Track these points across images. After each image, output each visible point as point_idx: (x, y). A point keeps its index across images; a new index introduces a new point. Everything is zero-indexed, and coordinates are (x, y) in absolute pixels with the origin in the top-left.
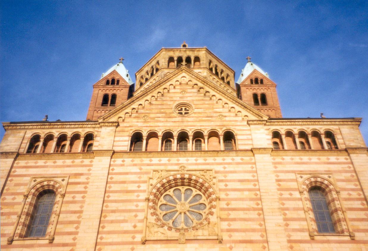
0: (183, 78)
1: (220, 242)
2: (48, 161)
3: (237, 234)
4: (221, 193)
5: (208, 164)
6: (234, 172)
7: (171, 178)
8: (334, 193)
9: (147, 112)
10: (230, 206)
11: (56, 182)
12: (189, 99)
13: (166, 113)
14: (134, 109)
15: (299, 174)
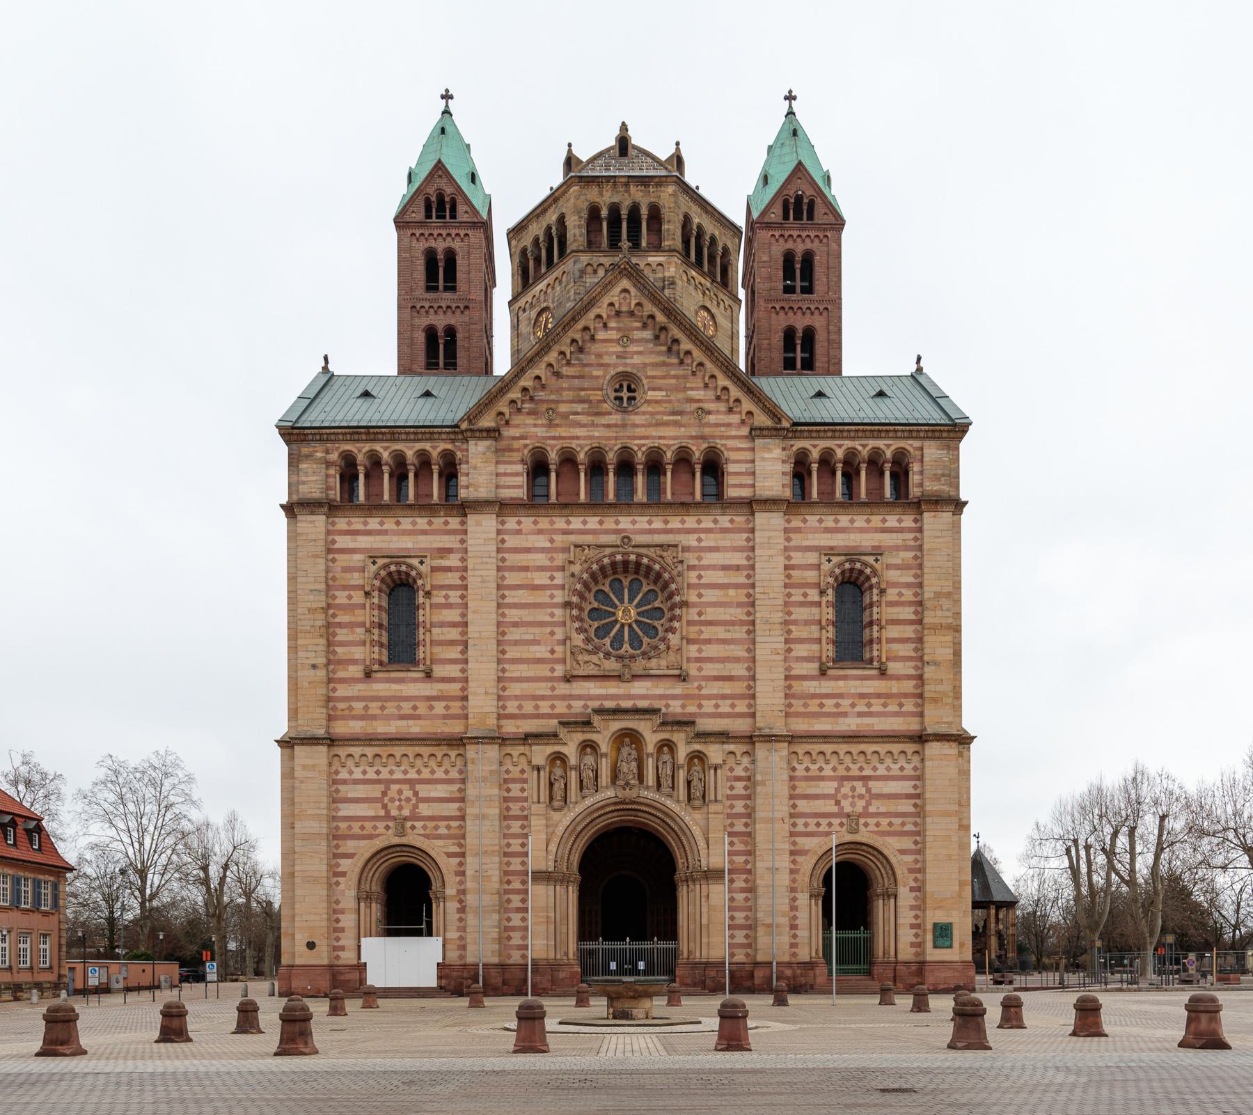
0: (623, 295)
1: (684, 680)
2: (384, 520)
3: (710, 665)
4: (691, 591)
5: (670, 531)
6: (716, 549)
7: (606, 561)
8: (875, 591)
9: (553, 397)
10: (703, 618)
11: (410, 566)
12: (637, 360)
13: (590, 402)
14: (525, 390)
15: (825, 555)
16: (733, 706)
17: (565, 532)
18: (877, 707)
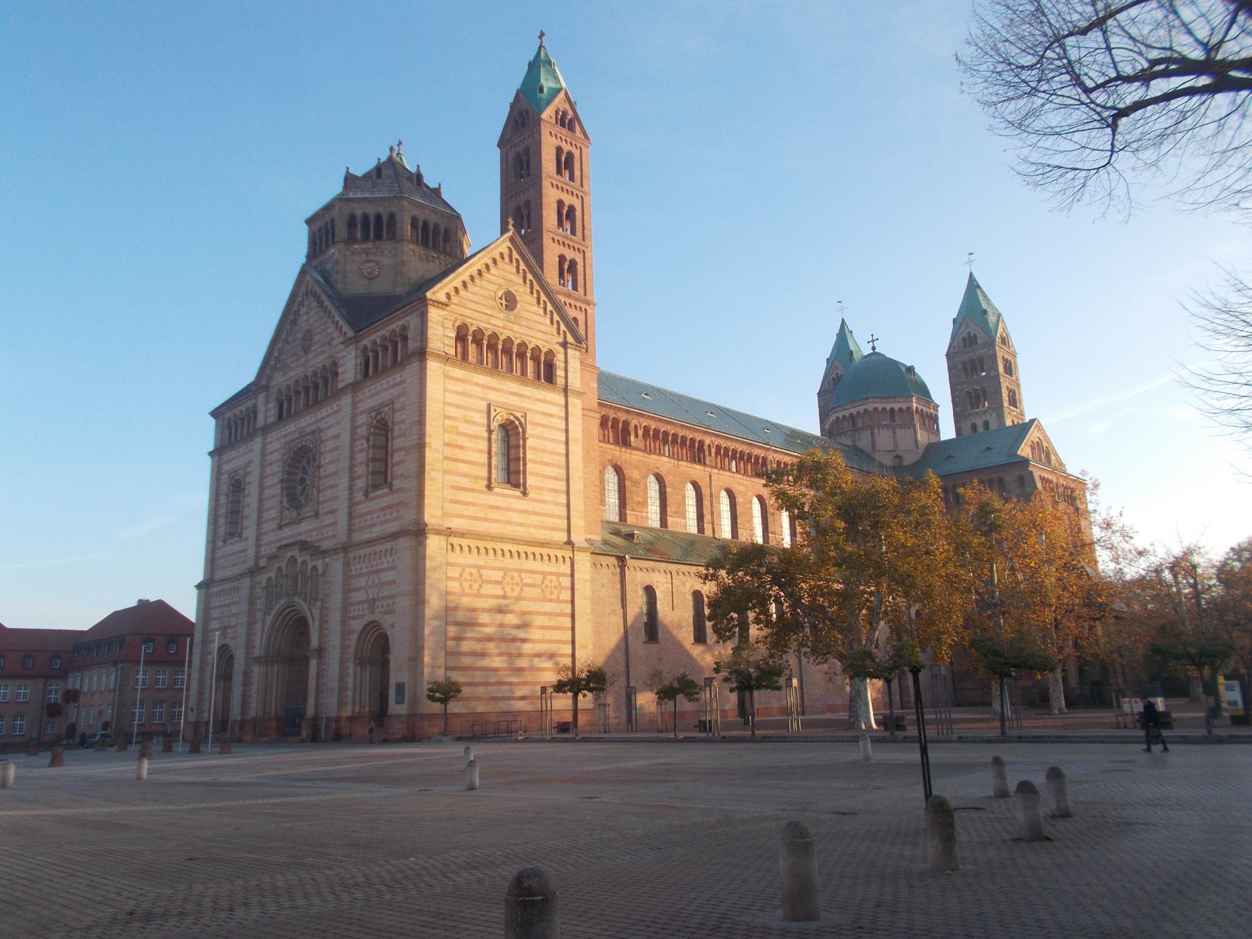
14: (276, 358)
16: (334, 530)
17: (285, 436)
18: (388, 517)
